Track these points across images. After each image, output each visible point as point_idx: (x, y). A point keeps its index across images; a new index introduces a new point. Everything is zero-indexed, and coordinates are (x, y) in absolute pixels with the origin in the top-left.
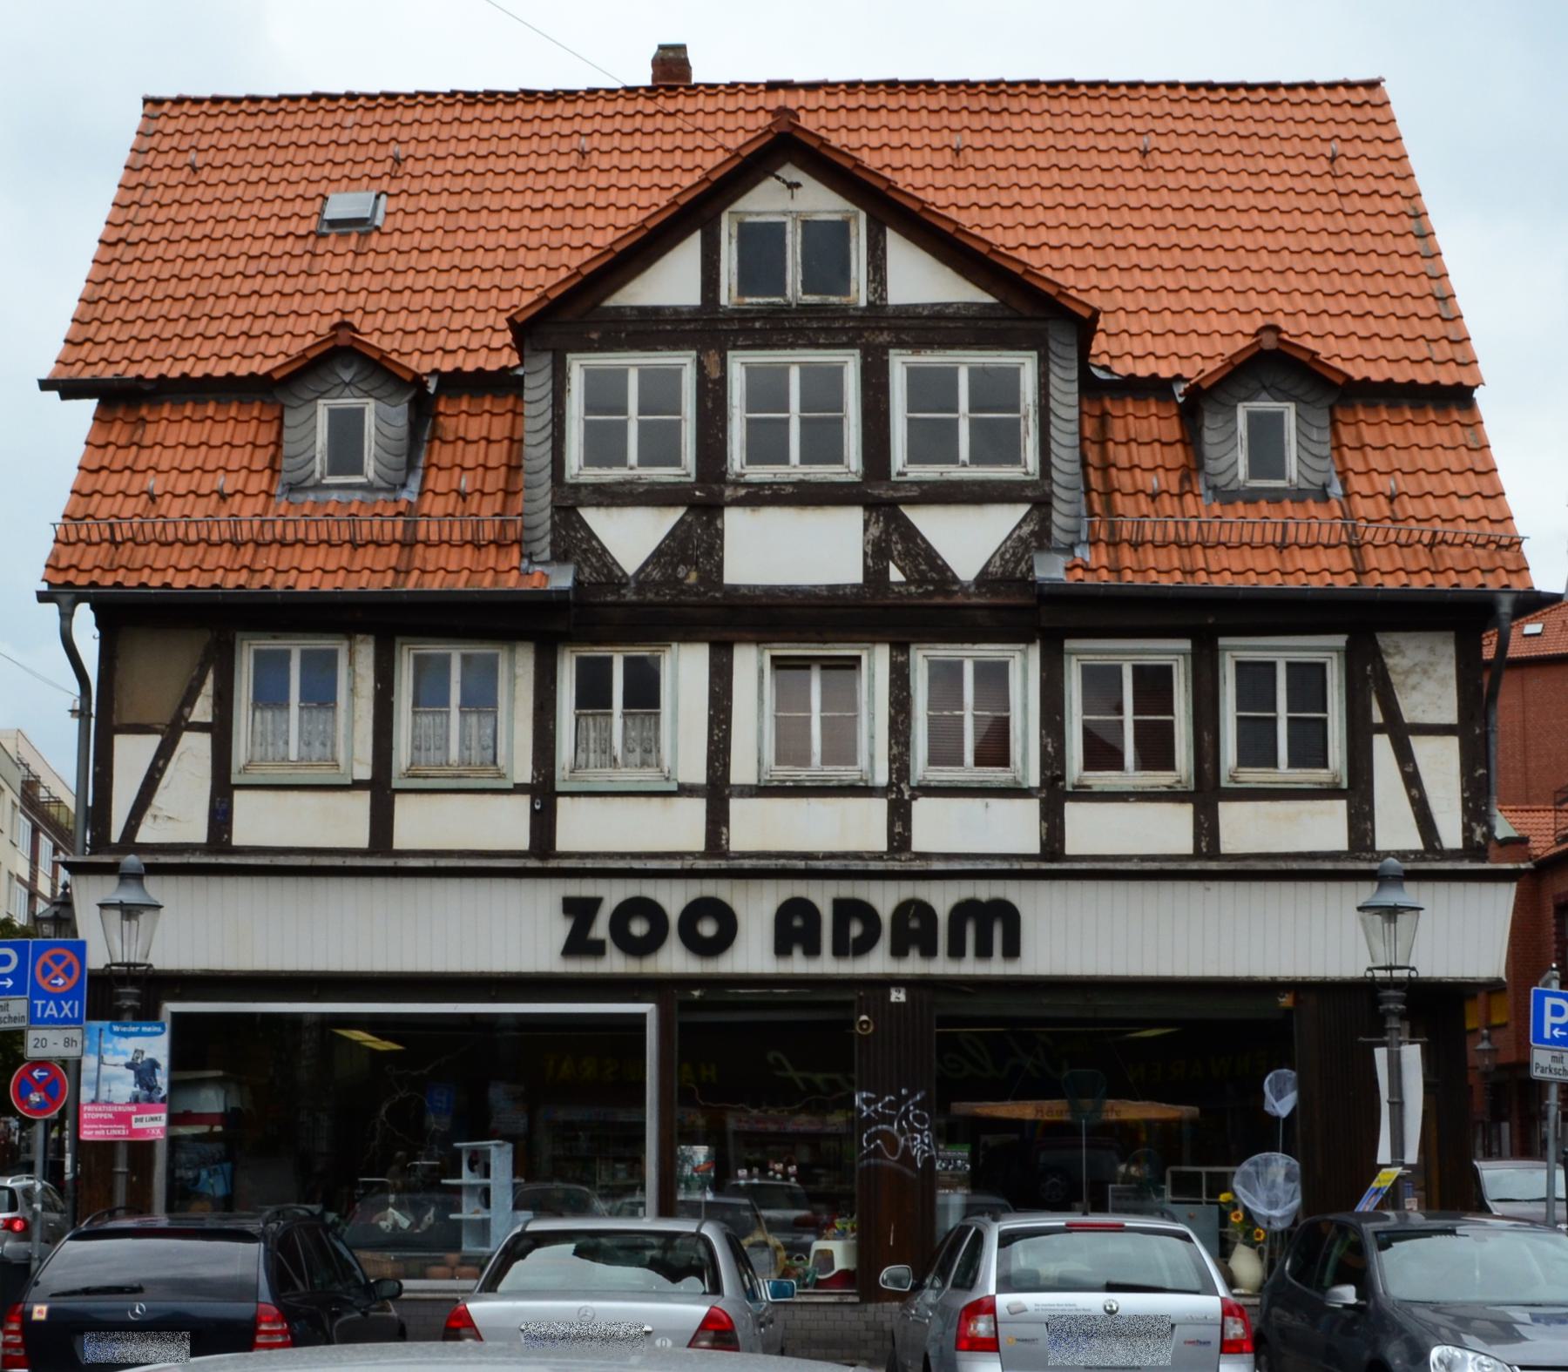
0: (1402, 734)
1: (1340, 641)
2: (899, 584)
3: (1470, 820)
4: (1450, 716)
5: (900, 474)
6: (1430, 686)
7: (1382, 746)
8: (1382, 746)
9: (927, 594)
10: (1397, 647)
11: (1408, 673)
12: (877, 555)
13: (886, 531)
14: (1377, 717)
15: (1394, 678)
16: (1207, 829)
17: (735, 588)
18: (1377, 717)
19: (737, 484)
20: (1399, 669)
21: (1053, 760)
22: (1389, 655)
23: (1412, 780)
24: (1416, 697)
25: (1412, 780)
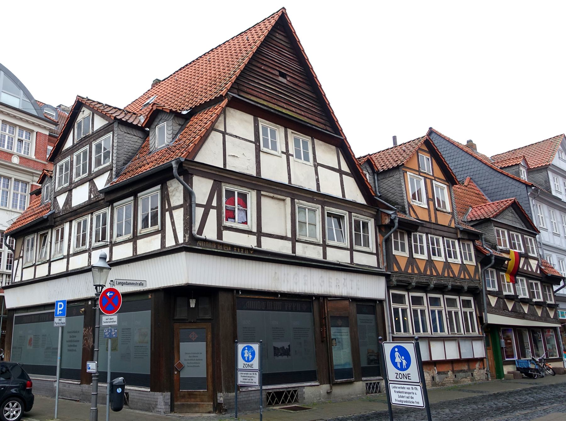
0: (171, 209)
1: (159, 187)
2: (93, 198)
3: (185, 233)
4: (181, 202)
5: (93, 171)
6: (177, 194)
7: (167, 214)
8: (167, 214)
9: (96, 199)
10: (171, 184)
11: (173, 191)
12: (90, 192)
13: (92, 187)
14: (167, 207)
15: (170, 194)
16: (135, 249)
17: (73, 207)
18: (167, 207)
19: (74, 183)
20: (171, 191)
21: (111, 236)
22: (169, 187)
23: (173, 224)
24: (175, 198)
25: (173, 224)
